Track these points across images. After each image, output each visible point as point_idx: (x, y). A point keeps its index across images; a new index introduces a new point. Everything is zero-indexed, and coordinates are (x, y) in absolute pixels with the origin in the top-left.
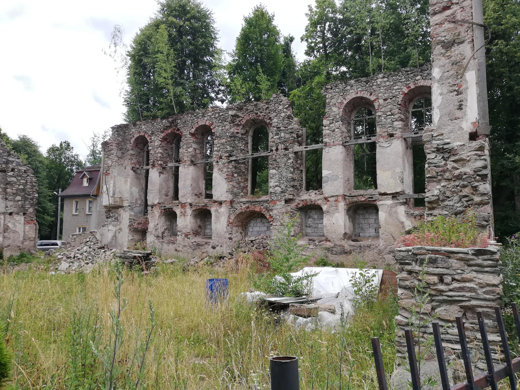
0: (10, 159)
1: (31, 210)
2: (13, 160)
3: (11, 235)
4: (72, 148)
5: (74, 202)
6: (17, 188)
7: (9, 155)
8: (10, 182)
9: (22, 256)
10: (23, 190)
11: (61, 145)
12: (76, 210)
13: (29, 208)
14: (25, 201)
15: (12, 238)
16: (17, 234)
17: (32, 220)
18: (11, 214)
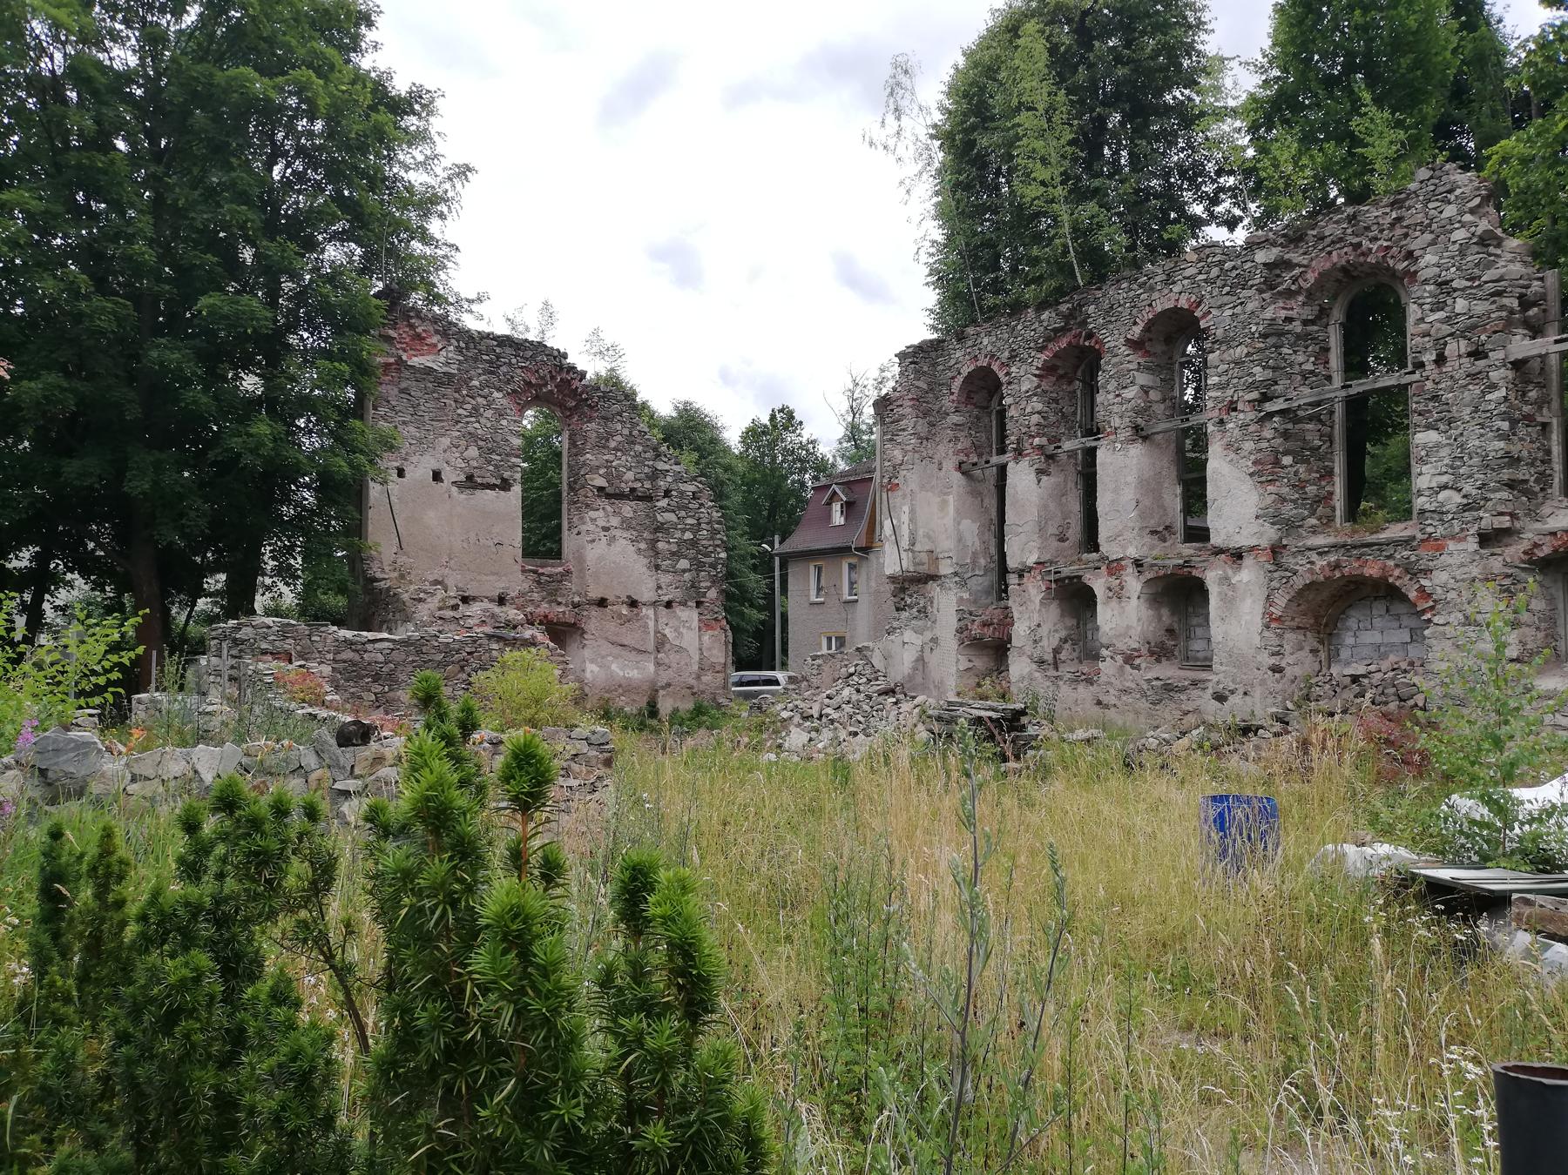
0: (661, 466)
1: (712, 594)
2: (667, 467)
3: (673, 658)
4: (801, 423)
5: (812, 568)
7: (658, 456)
9: (699, 711)
10: (693, 543)
11: (773, 418)
12: (819, 589)
13: (709, 588)
14: (698, 571)
15: (674, 665)
16: (685, 654)
17: (716, 619)
18: (669, 605)
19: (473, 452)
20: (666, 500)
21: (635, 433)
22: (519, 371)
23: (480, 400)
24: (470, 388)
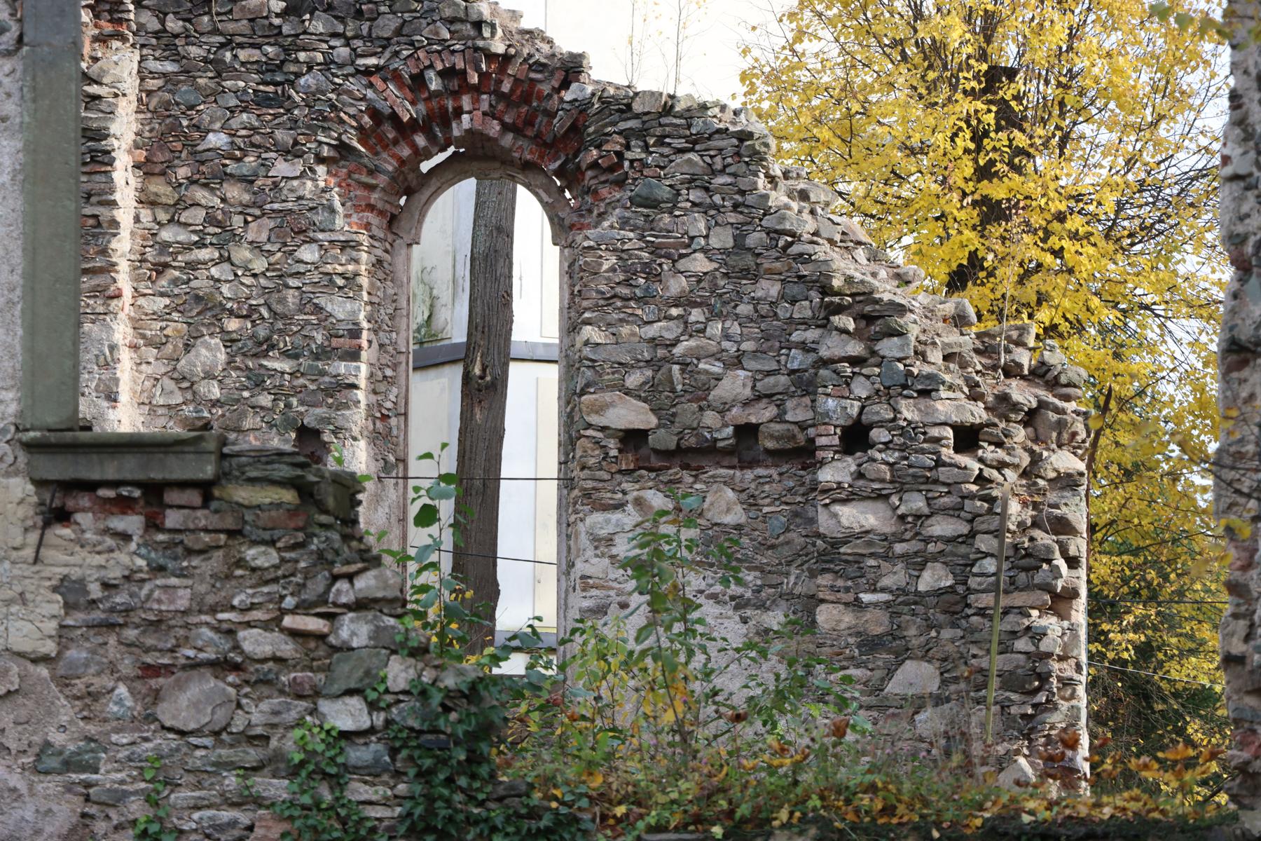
6: (902, 591)
8: (835, 544)
19: (211, 353)
20: (850, 464)
21: (755, 238)
22: (354, 85)
23: (234, 192)
24: (199, 159)
